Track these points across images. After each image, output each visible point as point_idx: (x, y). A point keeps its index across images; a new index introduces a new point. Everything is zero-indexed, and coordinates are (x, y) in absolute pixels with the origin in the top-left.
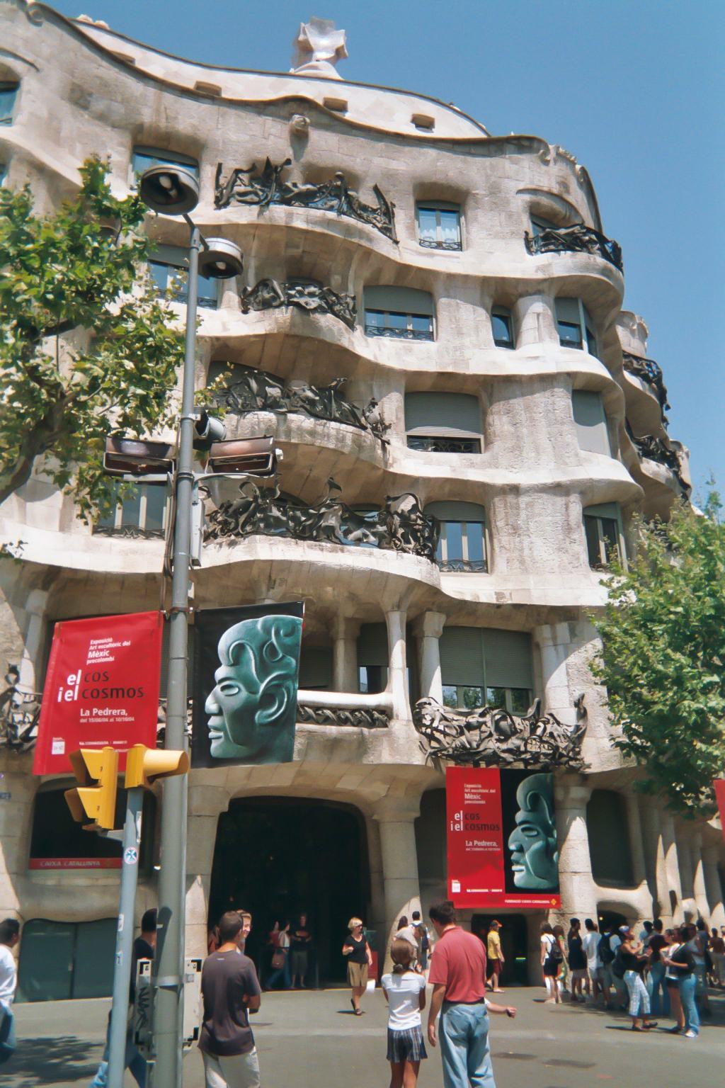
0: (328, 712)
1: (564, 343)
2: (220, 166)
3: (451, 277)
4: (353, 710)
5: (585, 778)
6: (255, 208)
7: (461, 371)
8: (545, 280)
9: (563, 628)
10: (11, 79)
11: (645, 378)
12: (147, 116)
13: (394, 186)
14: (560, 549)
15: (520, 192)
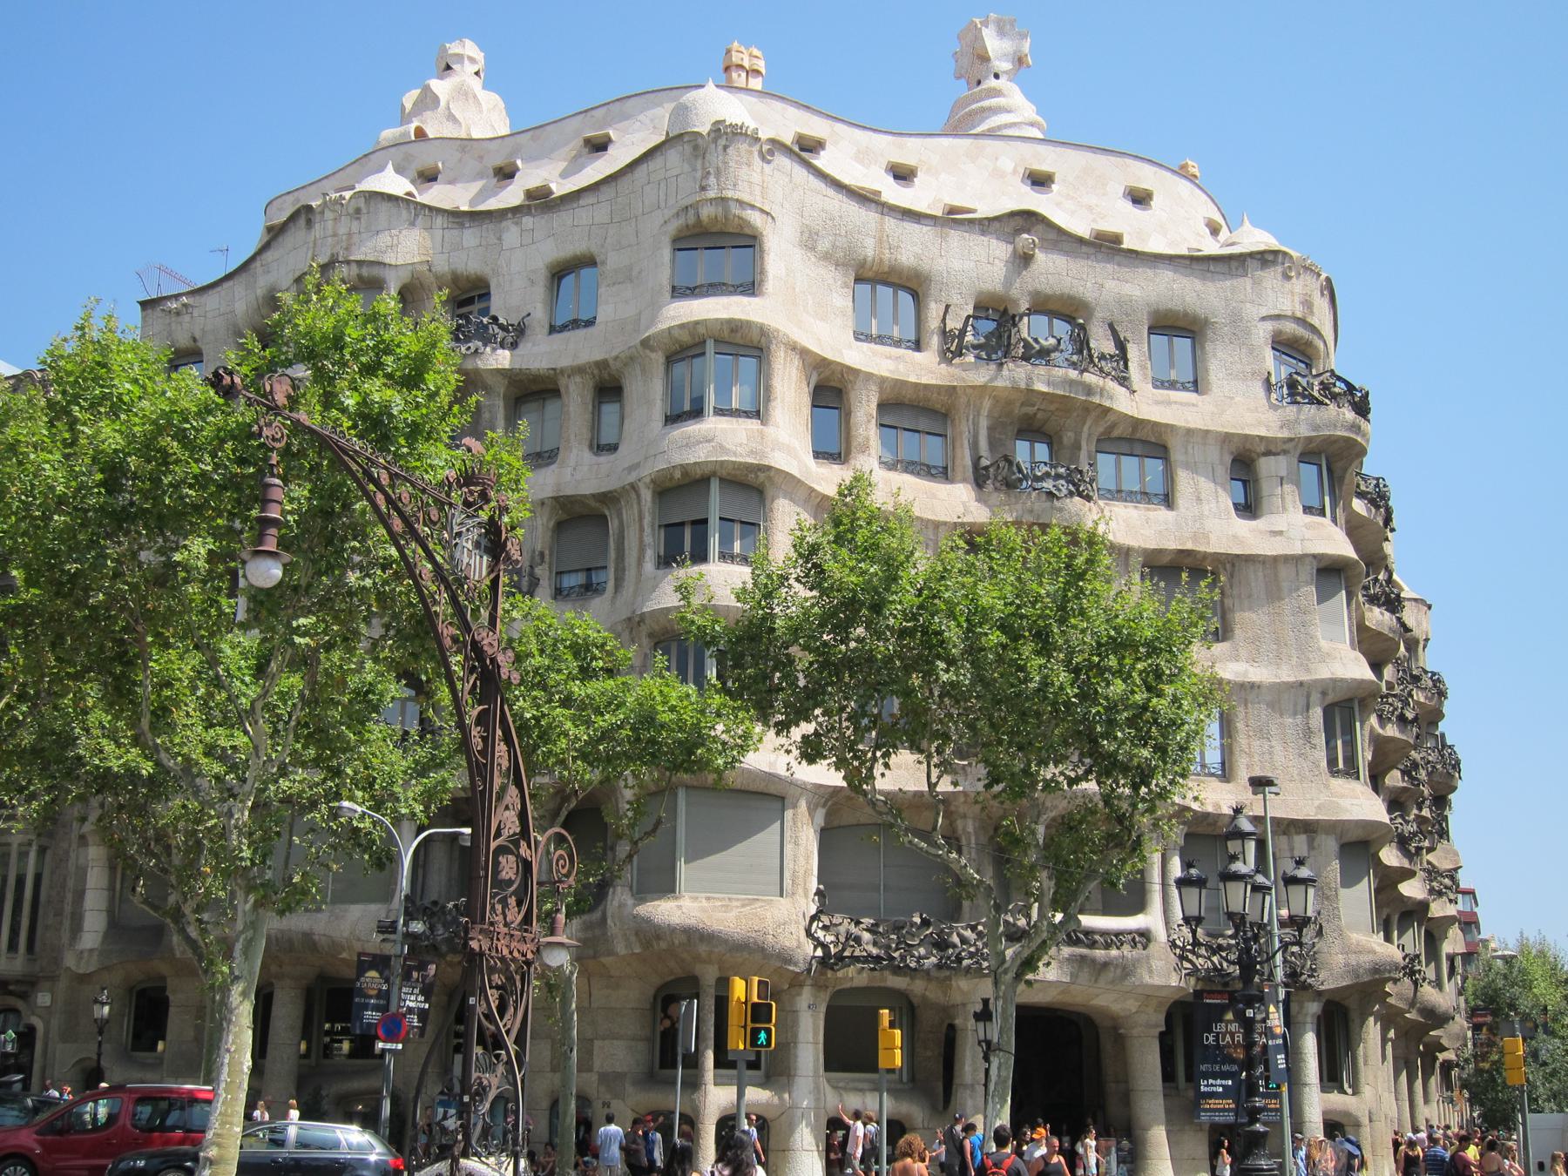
0: (1097, 937)
1: (1308, 510)
2: (947, 307)
3: (1190, 432)
4: (1117, 934)
5: (1320, 994)
6: (993, 366)
7: (1202, 548)
8: (1291, 440)
9: (1300, 841)
10: (747, 231)
11: (1373, 502)
12: (869, 249)
13: (1127, 315)
14: (1300, 755)
15: (1263, 319)
